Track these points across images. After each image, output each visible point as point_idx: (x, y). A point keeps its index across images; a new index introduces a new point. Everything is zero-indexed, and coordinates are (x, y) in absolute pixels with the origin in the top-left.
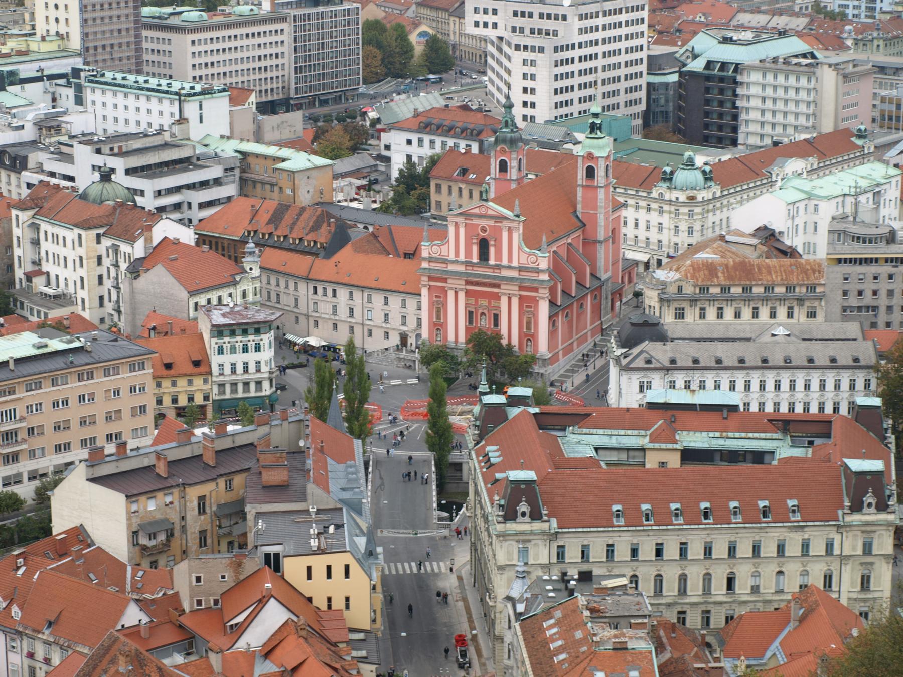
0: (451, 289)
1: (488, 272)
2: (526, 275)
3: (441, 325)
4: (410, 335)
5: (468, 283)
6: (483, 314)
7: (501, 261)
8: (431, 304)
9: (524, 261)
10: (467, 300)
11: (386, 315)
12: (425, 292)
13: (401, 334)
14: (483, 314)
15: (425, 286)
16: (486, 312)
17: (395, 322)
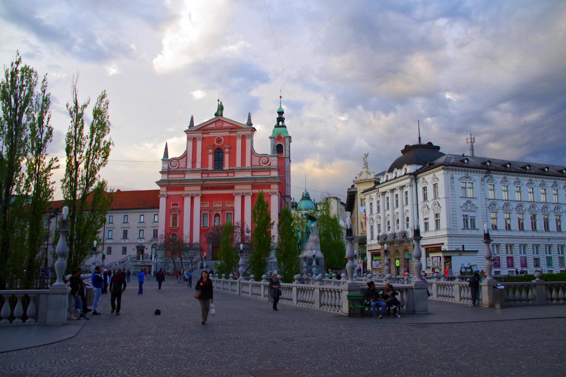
0: (188, 195)
1: (223, 176)
2: (257, 175)
3: (176, 230)
4: (146, 246)
5: (203, 188)
6: (217, 215)
7: (235, 165)
8: (168, 211)
9: (256, 162)
10: (202, 204)
11: (125, 233)
12: (163, 202)
13: (138, 247)
14: (217, 215)
15: (163, 196)
16: (220, 213)
17: (133, 236)
